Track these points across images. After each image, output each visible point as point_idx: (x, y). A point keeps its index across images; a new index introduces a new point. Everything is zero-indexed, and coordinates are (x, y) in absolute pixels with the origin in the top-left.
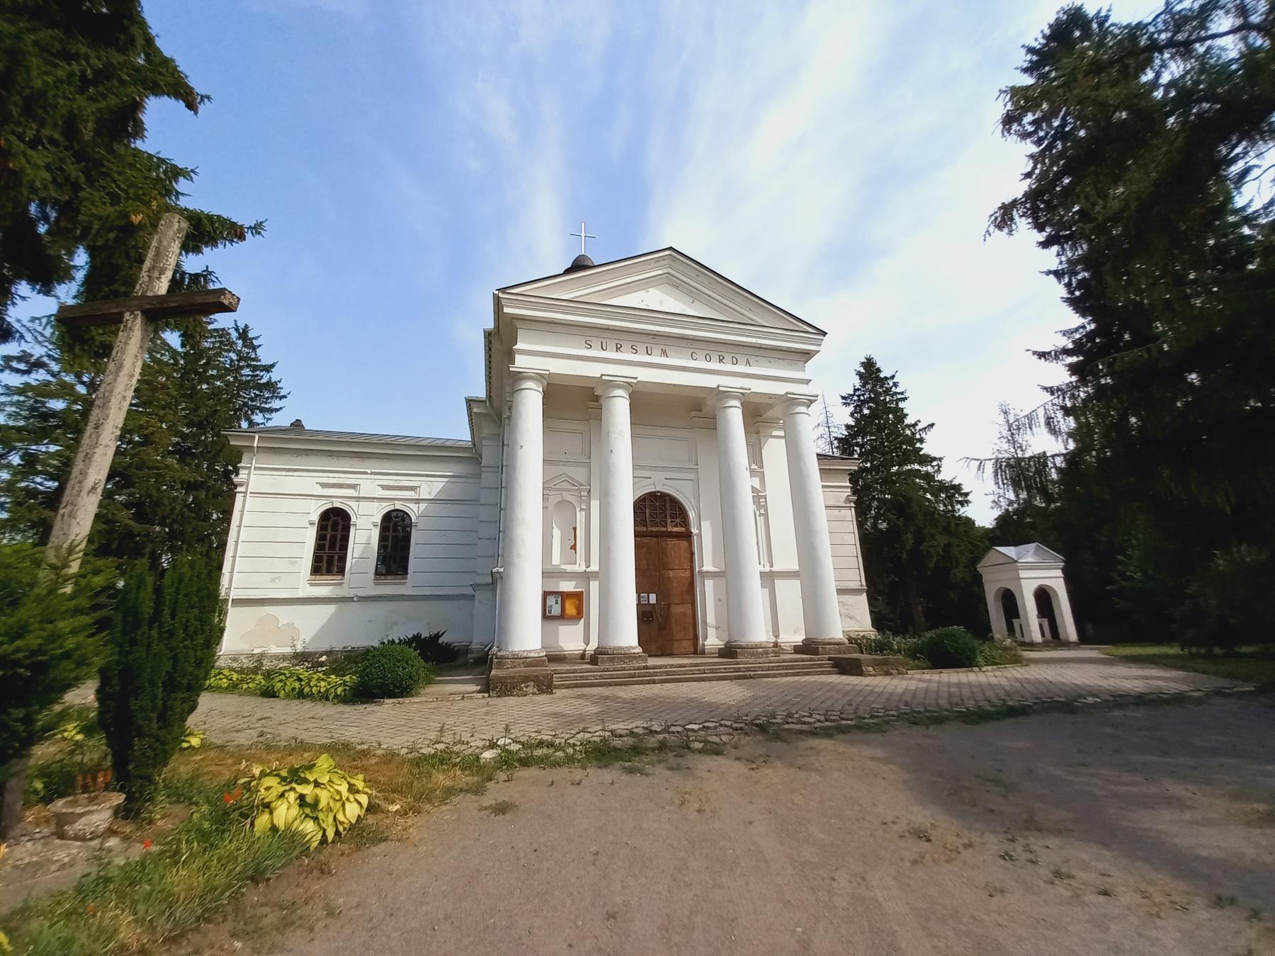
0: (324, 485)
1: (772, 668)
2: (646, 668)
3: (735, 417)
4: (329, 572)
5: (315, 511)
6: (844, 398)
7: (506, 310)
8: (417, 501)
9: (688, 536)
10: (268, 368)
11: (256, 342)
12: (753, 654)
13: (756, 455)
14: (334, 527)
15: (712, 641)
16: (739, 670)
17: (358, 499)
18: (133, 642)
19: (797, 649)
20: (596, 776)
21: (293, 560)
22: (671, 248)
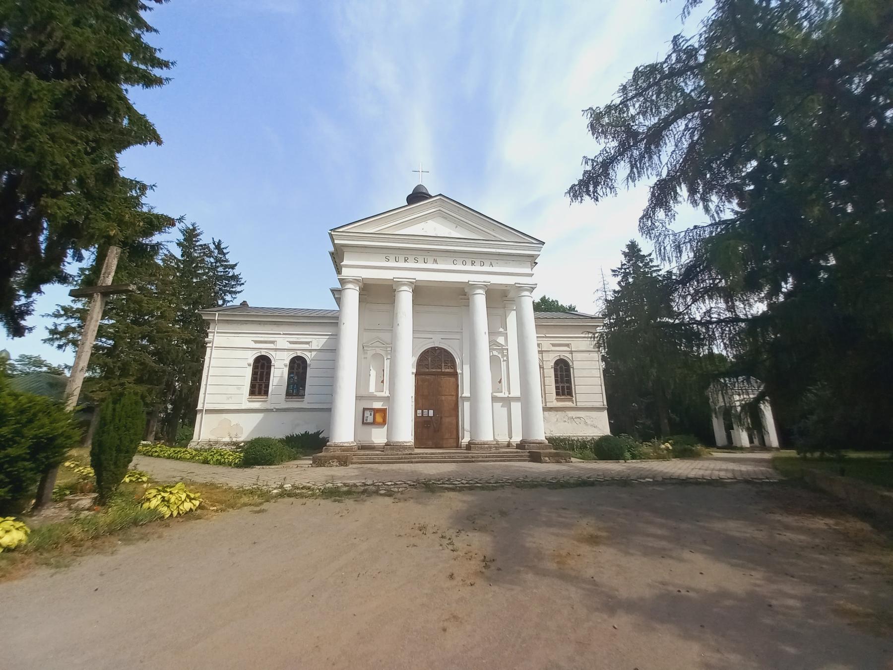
0: (256, 342)
1: (489, 457)
3: (480, 301)
4: (260, 394)
5: (251, 357)
6: (613, 271)
7: (336, 242)
8: (310, 351)
9: (455, 375)
10: (233, 267)
11: (225, 251)
12: (481, 448)
14: (262, 366)
15: (465, 440)
16: (467, 457)
17: (276, 350)
18: (103, 432)
20: (327, 504)
21: (239, 387)
22: (440, 195)
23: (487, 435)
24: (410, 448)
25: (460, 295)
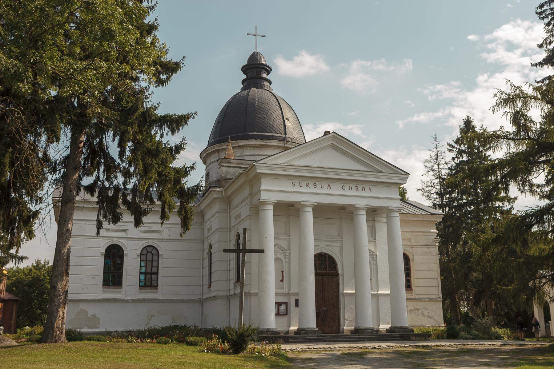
2: (321, 336)
3: (362, 219)
13: (373, 235)
14: (114, 255)
22: (334, 132)
24: (315, 332)
25: (345, 213)
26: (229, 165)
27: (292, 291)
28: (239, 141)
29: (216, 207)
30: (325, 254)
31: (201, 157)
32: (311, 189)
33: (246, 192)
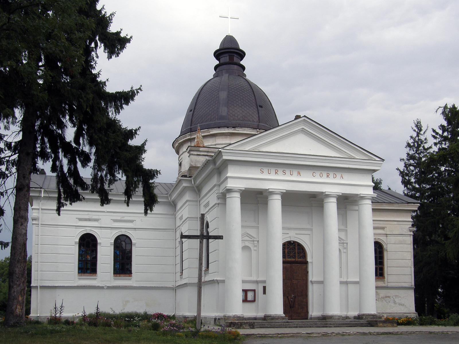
2: (287, 322)
14: (88, 244)
19: (355, 318)
23: (335, 309)
24: (282, 318)
26: (199, 153)
27: (260, 279)
28: (210, 130)
29: (187, 197)
30: (295, 242)
31: (173, 147)
32: (281, 177)
33: (214, 181)
